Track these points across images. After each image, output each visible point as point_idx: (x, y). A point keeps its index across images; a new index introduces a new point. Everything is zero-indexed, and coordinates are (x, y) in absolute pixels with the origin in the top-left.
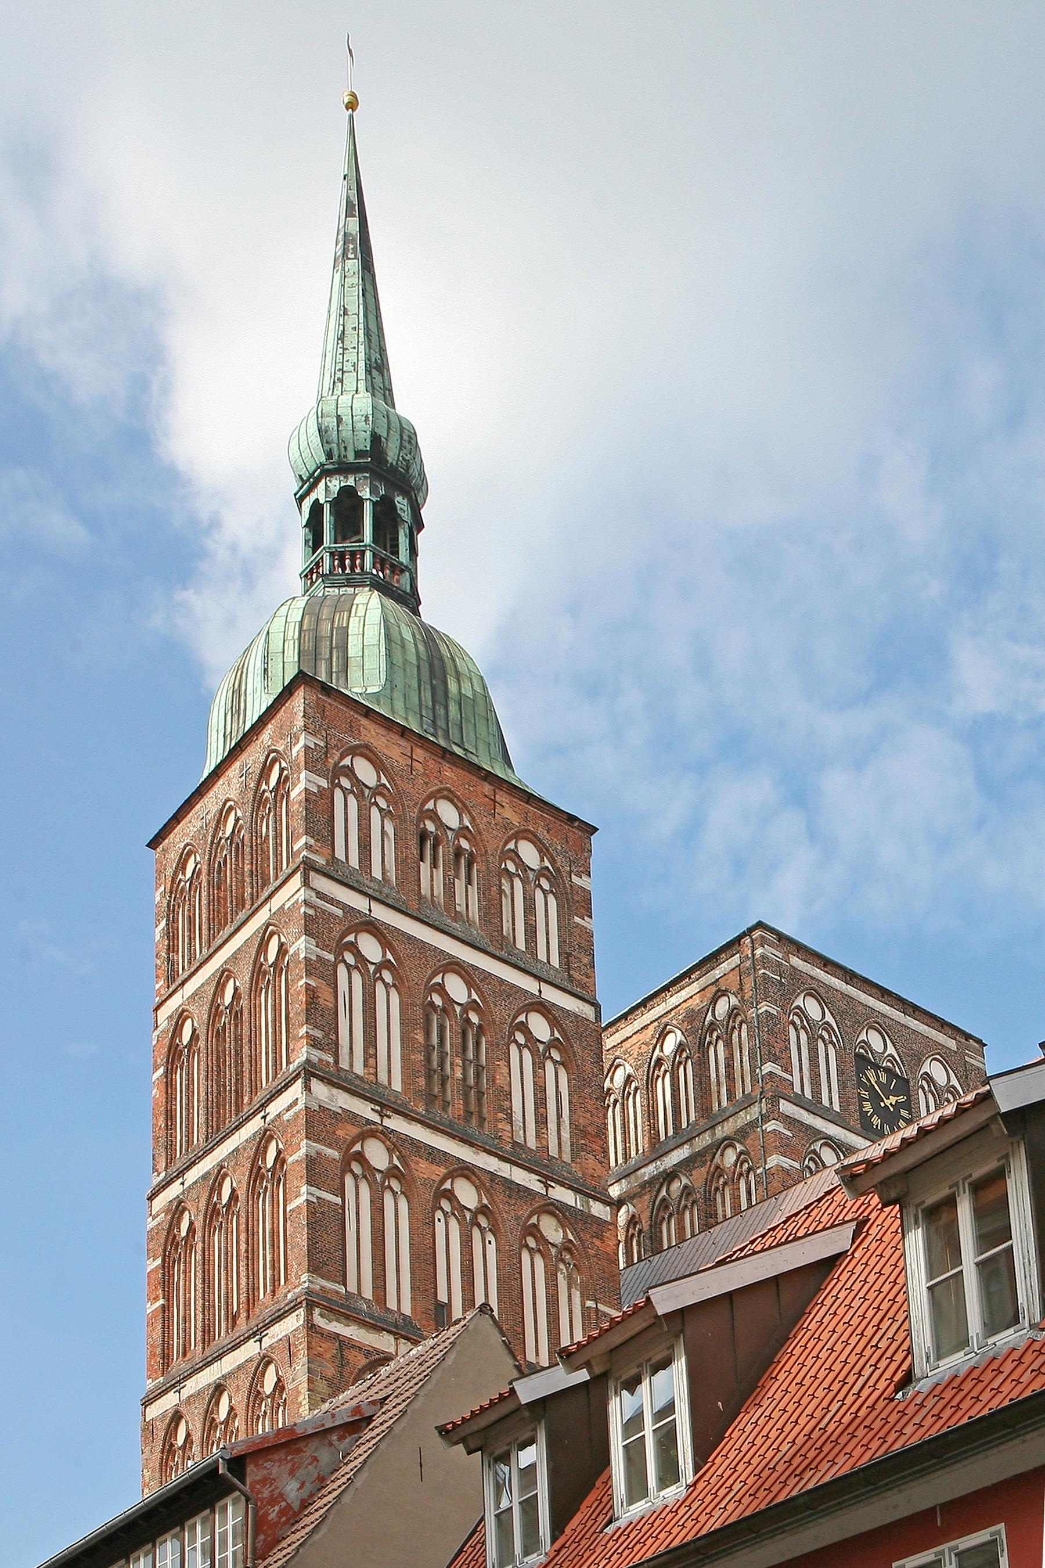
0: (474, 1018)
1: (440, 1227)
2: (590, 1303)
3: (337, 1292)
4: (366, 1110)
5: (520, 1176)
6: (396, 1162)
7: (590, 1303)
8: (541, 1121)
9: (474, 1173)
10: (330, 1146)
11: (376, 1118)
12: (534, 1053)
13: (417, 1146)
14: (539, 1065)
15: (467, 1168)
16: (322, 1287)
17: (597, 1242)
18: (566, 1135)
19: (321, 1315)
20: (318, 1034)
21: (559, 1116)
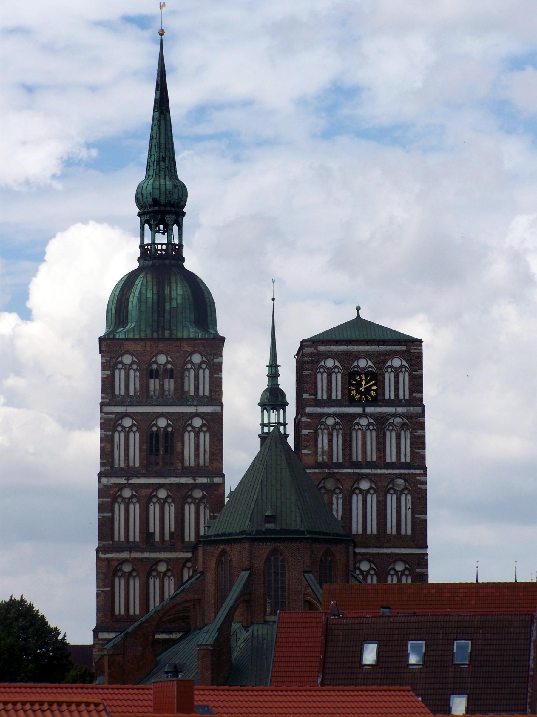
0: (170, 429)
1: (151, 508)
2: (212, 514)
3: (109, 544)
4: (122, 481)
5: (183, 480)
6: (134, 493)
7: (212, 514)
8: (197, 456)
9: (164, 486)
10: (107, 498)
11: (126, 482)
12: (195, 432)
13: (140, 486)
14: (197, 436)
15: (162, 485)
16: (104, 545)
17: (215, 492)
18: (207, 456)
19: (102, 554)
20: (105, 461)
21: (205, 450)
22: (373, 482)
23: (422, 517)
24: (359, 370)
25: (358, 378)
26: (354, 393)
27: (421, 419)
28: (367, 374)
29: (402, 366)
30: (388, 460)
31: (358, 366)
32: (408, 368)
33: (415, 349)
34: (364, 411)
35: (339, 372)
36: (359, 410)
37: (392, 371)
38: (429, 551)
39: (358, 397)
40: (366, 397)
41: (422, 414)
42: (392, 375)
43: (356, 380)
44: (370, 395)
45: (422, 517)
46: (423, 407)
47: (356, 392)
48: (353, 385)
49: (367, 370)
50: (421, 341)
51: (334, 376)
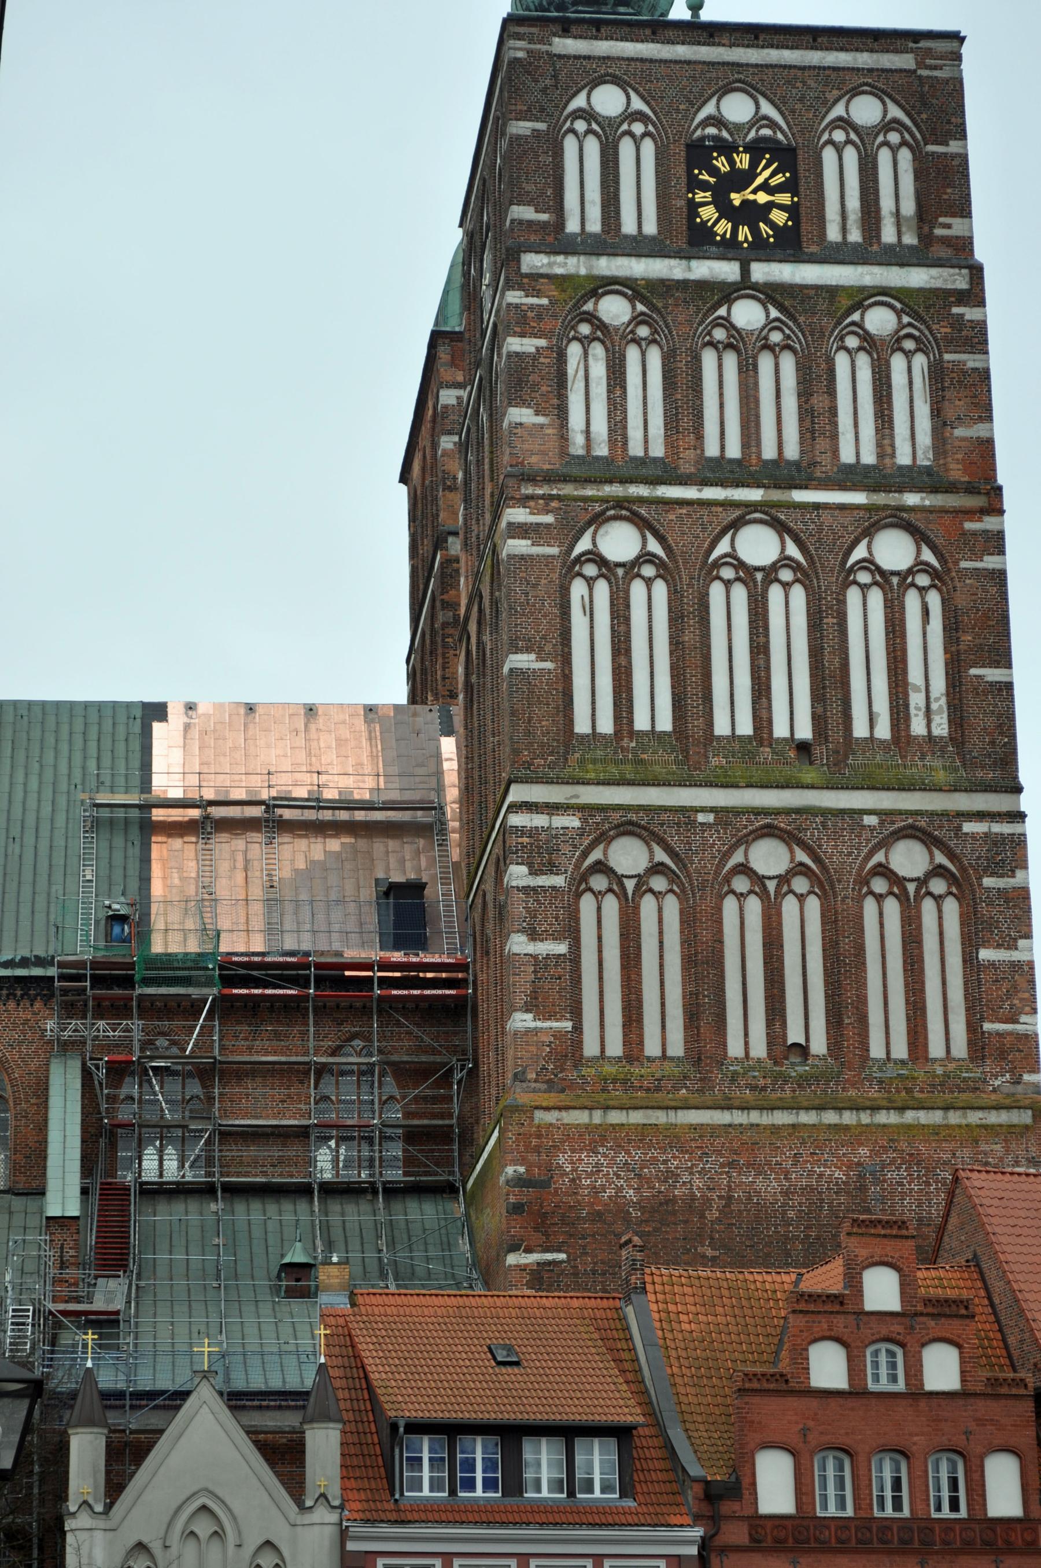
22: (790, 532)
23: (992, 674)
24: (725, 134)
25: (722, 164)
26: (708, 213)
27: (970, 314)
28: (756, 150)
29: (888, 125)
30: (847, 456)
31: (717, 121)
32: (907, 129)
33: (935, 68)
34: (745, 272)
35: (646, 134)
36: (728, 271)
37: (849, 141)
38: (1025, 801)
39: (723, 227)
40: (755, 231)
41: (975, 295)
42: (851, 156)
43: (714, 171)
44: (772, 225)
45: (992, 674)
46: (977, 272)
47: (718, 210)
48: (704, 186)
49: (752, 134)
50: (957, 38)
51: (626, 147)
